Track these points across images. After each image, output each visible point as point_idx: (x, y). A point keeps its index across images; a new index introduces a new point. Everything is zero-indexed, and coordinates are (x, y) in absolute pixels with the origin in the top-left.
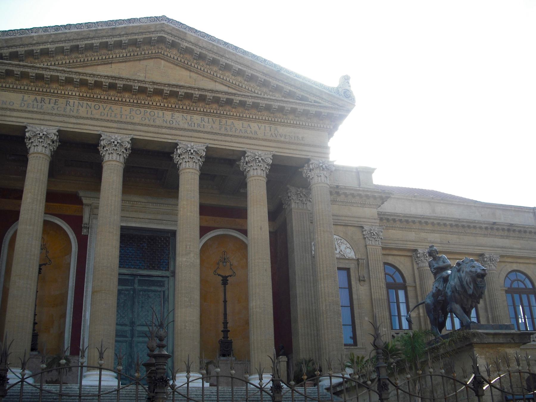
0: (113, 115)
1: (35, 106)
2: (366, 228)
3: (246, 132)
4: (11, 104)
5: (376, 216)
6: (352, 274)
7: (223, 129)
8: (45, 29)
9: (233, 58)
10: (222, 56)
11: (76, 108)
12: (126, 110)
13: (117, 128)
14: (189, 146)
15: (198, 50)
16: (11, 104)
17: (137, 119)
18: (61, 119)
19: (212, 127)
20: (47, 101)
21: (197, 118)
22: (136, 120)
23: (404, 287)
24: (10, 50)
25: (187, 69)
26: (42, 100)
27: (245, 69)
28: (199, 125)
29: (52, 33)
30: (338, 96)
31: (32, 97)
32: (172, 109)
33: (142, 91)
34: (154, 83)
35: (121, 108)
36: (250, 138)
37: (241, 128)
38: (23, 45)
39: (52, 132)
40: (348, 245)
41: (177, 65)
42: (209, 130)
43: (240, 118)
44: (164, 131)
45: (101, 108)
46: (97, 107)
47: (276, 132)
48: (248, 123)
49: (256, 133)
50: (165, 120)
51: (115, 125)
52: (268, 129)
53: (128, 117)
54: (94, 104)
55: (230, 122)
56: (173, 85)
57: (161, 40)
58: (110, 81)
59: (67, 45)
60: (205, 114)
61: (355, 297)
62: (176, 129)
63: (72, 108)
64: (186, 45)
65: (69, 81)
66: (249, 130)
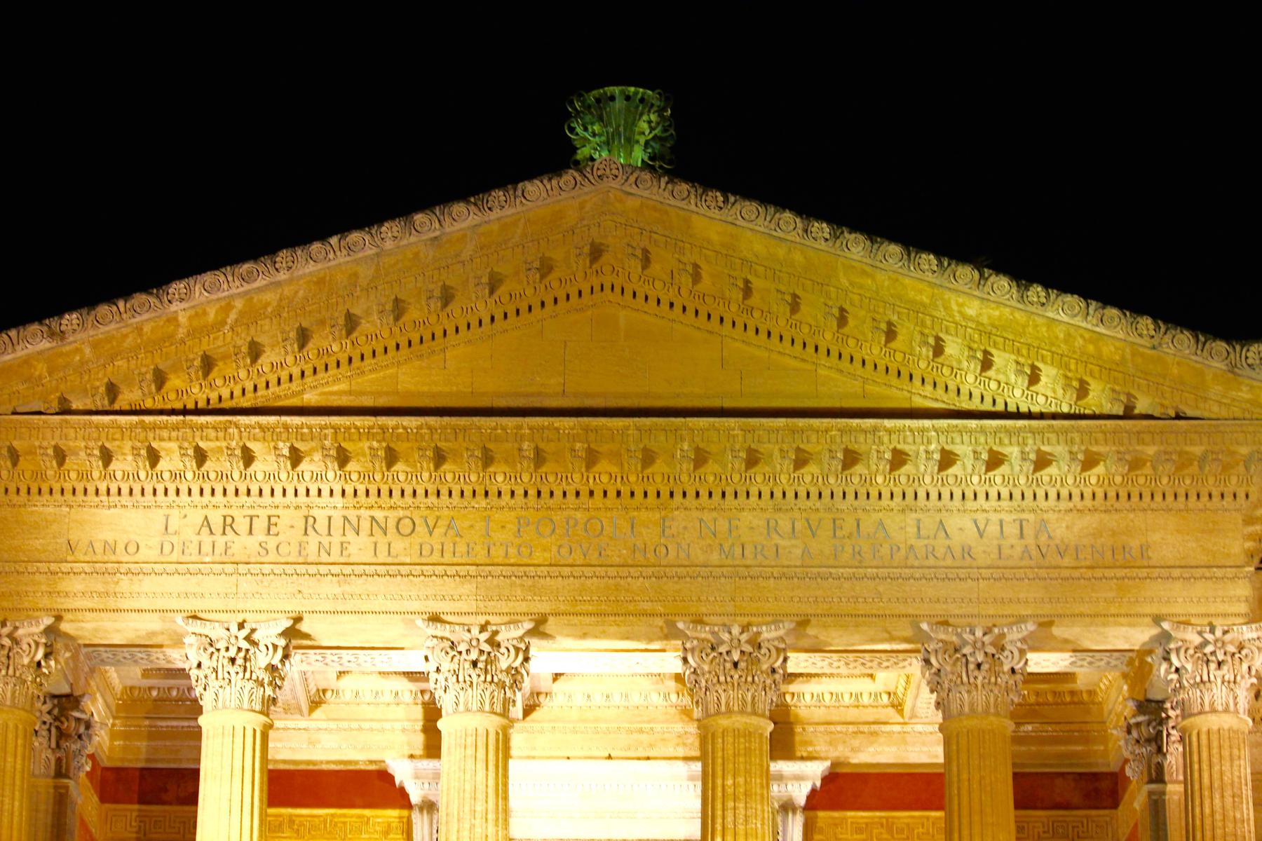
0: (461, 548)
1: (207, 548)
4: (132, 549)
7: (849, 549)
11: (337, 538)
14: (726, 637)
16: (132, 549)
19: (806, 551)
29: (234, 291)
35: (488, 519)
37: (912, 541)
45: (421, 529)
46: (406, 526)
47: (1043, 539)
48: (938, 517)
50: (640, 544)
53: (512, 551)
54: (394, 516)
63: (325, 540)
66: (941, 542)
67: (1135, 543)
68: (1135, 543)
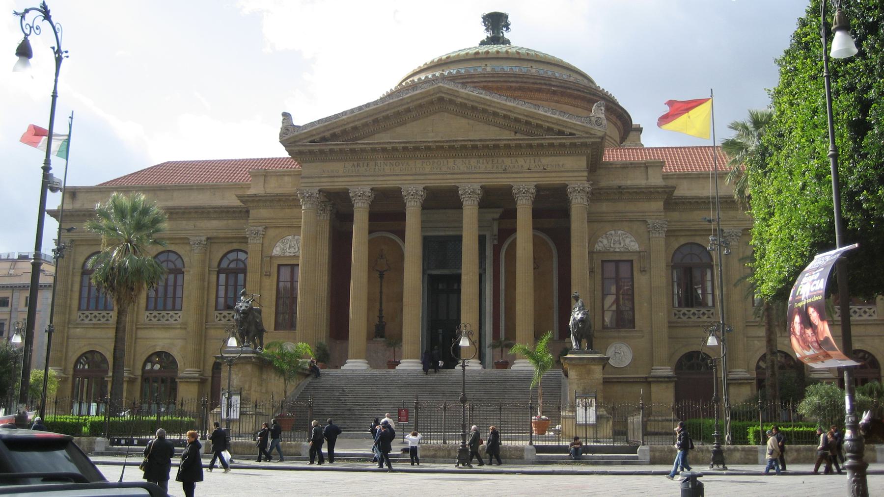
2: (649, 221)
3: (514, 167)
5: (662, 208)
6: (635, 265)
8: (352, 111)
9: (498, 106)
10: (489, 106)
12: (419, 163)
13: (412, 181)
15: (470, 104)
17: (427, 170)
18: (371, 178)
20: (361, 165)
21: (473, 162)
22: (427, 170)
23: (711, 267)
24: (331, 132)
25: (465, 117)
26: (358, 165)
27: (509, 114)
28: (475, 167)
30: (589, 126)
31: (351, 164)
32: (454, 157)
33: (428, 148)
34: (435, 142)
36: (517, 173)
38: (339, 127)
39: (367, 189)
40: (633, 239)
41: (457, 115)
42: (482, 170)
43: (509, 156)
44: (449, 176)
49: (522, 166)
51: (411, 178)
52: (532, 161)
55: (500, 160)
56: (450, 141)
57: (441, 100)
58: (403, 145)
59: (370, 120)
60: (480, 157)
61: (636, 285)
62: (457, 174)
64: (460, 100)
65: (374, 150)
67: (561, 163)
68: (561, 163)
